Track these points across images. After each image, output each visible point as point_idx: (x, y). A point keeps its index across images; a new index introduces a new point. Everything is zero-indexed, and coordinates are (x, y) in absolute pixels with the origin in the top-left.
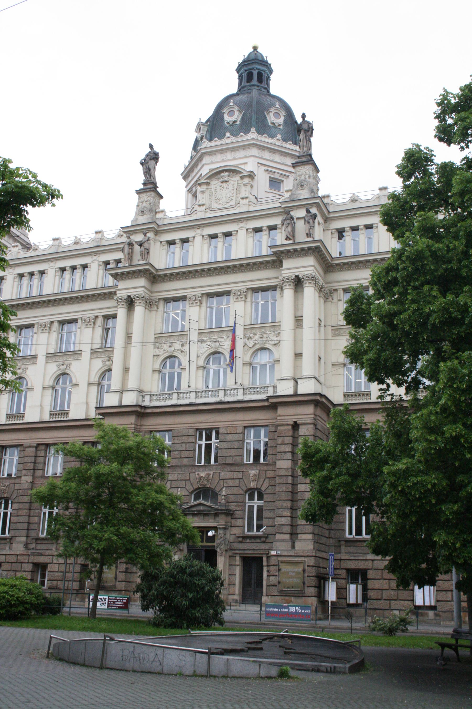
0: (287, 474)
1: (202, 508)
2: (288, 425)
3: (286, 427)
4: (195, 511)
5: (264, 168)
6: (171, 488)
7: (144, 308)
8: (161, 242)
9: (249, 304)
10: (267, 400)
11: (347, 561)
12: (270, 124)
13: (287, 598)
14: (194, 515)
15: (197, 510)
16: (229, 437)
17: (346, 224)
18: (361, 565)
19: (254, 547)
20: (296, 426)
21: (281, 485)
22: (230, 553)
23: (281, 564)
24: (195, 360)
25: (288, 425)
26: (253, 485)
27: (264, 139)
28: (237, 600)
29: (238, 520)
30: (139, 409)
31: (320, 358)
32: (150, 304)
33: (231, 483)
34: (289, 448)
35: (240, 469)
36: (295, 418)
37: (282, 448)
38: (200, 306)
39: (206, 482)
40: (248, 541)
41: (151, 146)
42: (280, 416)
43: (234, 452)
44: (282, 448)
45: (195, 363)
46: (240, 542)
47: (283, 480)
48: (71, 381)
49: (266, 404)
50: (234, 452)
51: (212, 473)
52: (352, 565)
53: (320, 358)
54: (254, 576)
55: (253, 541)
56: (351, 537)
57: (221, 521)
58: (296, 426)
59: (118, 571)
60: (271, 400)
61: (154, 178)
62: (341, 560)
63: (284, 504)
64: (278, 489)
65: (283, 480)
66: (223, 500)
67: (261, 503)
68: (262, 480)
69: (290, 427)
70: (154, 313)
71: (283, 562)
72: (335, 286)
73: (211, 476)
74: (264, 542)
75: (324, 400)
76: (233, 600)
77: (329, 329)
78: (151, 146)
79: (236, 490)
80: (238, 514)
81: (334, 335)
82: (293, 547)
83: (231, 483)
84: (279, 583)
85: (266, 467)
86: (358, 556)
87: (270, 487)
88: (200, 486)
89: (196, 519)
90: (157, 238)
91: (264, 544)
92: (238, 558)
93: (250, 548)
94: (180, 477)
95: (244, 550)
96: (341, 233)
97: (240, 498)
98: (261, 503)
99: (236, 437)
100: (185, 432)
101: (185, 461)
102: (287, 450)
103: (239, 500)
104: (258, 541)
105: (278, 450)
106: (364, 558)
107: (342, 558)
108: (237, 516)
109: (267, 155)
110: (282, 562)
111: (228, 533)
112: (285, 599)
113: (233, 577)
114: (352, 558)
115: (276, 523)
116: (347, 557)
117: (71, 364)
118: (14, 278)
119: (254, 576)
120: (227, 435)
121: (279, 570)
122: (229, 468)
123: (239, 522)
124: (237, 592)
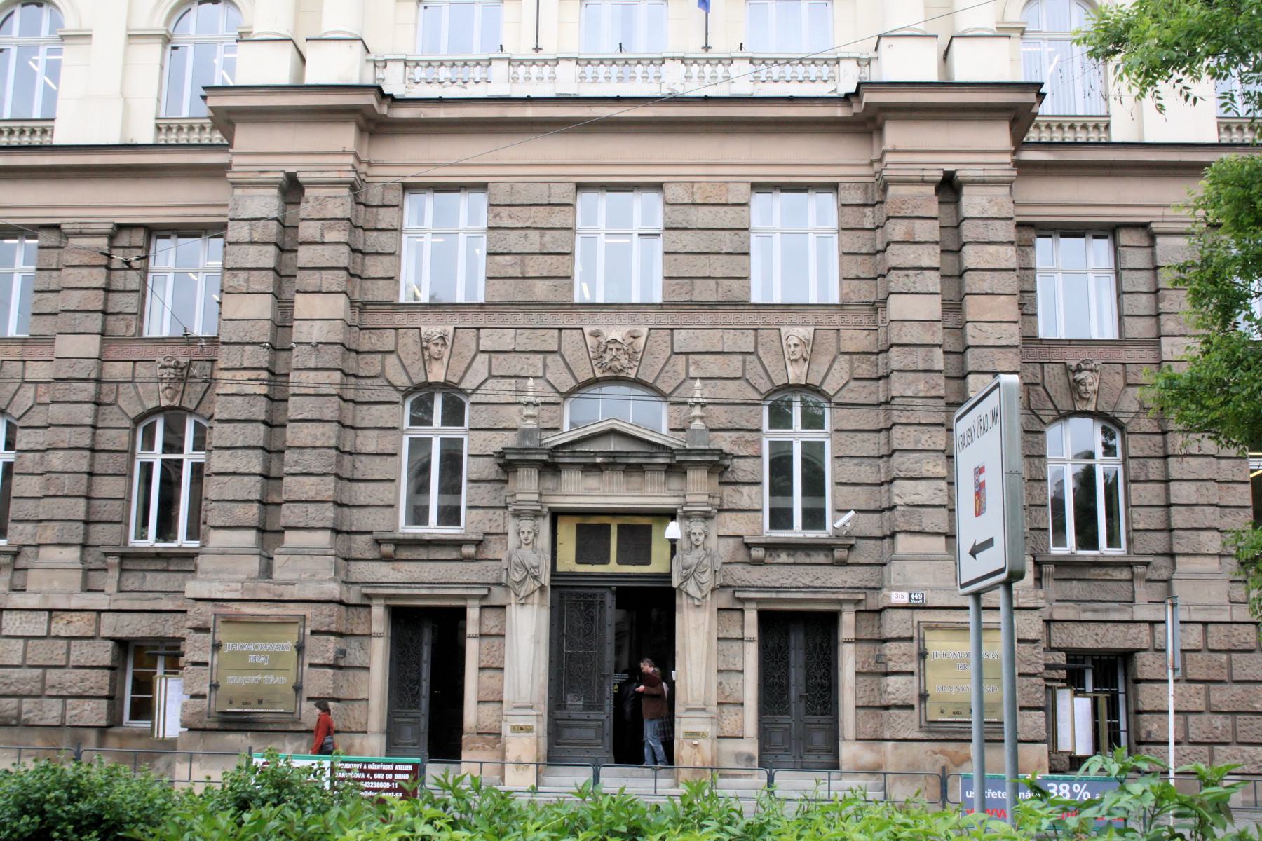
0: (928, 339)
2: (923, 182)
3: (915, 190)
4: (596, 454)
6: (491, 376)
10: (857, 94)
11: (1071, 625)
13: (951, 747)
14: (590, 468)
15: (605, 454)
16: (702, 217)
18: (1115, 639)
19: (807, 581)
20: (949, 187)
21: (911, 376)
22: (724, 600)
23: (929, 636)
25: (923, 182)
26: (795, 374)
28: (750, 758)
30: (370, 99)
33: (714, 366)
34: (930, 257)
35: (746, 319)
36: (949, 163)
37: (908, 256)
39: (624, 360)
40: (784, 557)
42: (894, 151)
43: (719, 266)
44: (908, 256)
46: (759, 563)
47: (917, 359)
48: (56, 23)
49: (839, 112)
50: (719, 266)
51: (644, 330)
52: (1085, 639)
54: (796, 675)
55: (801, 557)
56: (1114, 552)
57: (697, 488)
58: (949, 187)
59: (307, 661)
60: (868, 97)
63: (924, 438)
64: (898, 386)
65: (917, 359)
66: (698, 422)
68: (824, 361)
69: (931, 190)
71: (932, 627)
73: (642, 341)
74: (843, 563)
76: (738, 756)
79: (731, 390)
80: (742, 469)
83: (714, 366)
84: (923, 697)
85: (836, 318)
86: (1107, 610)
87: (853, 384)
88: (599, 375)
89: (593, 481)
91: (841, 570)
92: (751, 617)
93: (798, 583)
94: (525, 340)
95: (777, 589)
97: (740, 417)
99: (727, 217)
100: (538, 193)
101: (541, 291)
102: (926, 262)
103: (745, 425)
104: (820, 558)
105: (893, 262)
106: (1127, 618)
107: (1056, 617)
108: (741, 476)
110: (929, 629)
111: (714, 528)
112: (942, 752)
113: (734, 678)
114: (1088, 616)
115: (897, 500)
116: (1071, 615)
119: (796, 675)
120: (693, 209)
121: (923, 655)
122: (705, 318)
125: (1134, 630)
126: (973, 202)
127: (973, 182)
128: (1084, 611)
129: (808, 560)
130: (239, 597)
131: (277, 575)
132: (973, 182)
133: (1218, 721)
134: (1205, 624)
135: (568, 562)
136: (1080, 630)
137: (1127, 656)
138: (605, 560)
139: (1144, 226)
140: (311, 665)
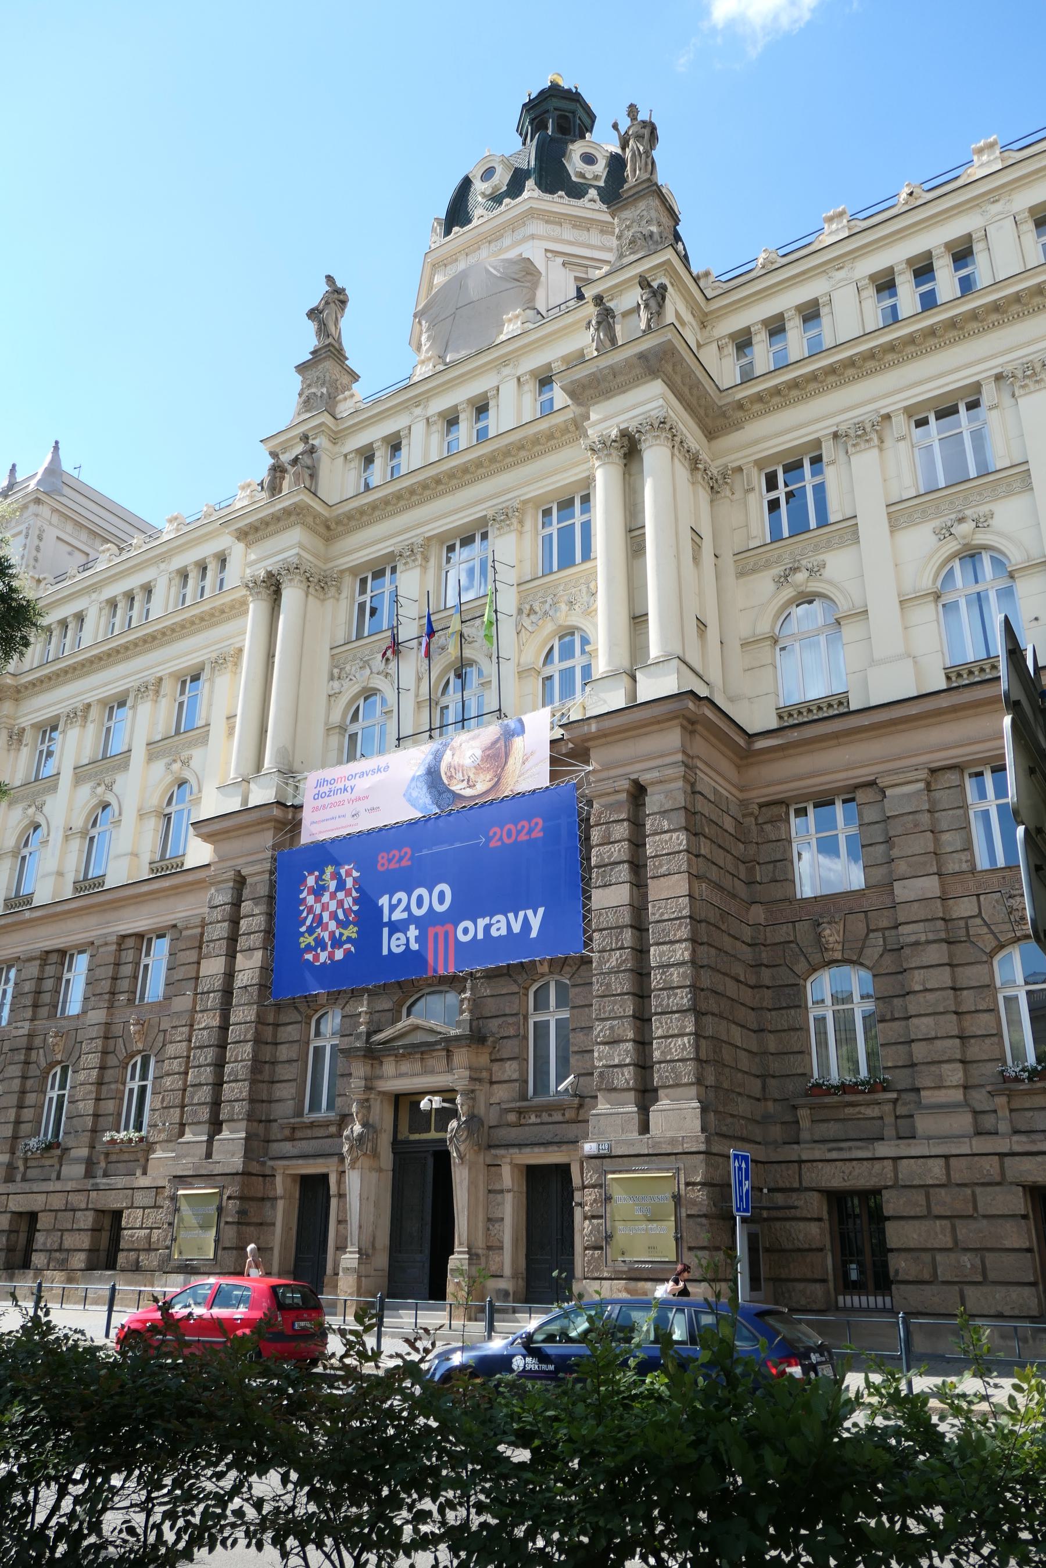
1: (419, 1037)
5: (560, 260)
7: (302, 594)
8: (345, 456)
9: (528, 537)
11: (820, 1165)
12: (574, 179)
15: (404, 1047)
17: (753, 316)
18: (861, 1177)
24: (413, 688)
27: (559, 203)
29: (508, 1064)
31: (702, 625)
32: (321, 584)
38: (424, 568)
41: (330, 279)
45: (412, 693)
53: (702, 625)
59: (223, 1220)
61: (339, 340)
62: (801, 1162)
67: (565, 1014)
70: (330, 603)
72: (734, 460)
75: (708, 712)
77: (728, 562)
78: (330, 279)
81: (741, 574)
82: (644, 1128)
86: (850, 1149)
90: (336, 449)
96: (743, 342)
98: (565, 1014)
106: (869, 1155)
107: (804, 1158)
109: (568, 233)
114: (834, 1155)
116: (817, 1155)
117: (190, 758)
118: (101, 610)
123: (510, 1070)
124: (507, 1271)
125: (878, 1165)
126: (653, 802)
127: (652, 784)
128: (830, 1150)
129: (550, 1120)
130: (191, 1173)
131: (216, 1157)
132: (652, 784)
133: (966, 1259)
134: (946, 1157)
135: (404, 1134)
136: (828, 1168)
137: (877, 1192)
138: (429, 1131)
139: (872, 784)
140: (227, 1223)
